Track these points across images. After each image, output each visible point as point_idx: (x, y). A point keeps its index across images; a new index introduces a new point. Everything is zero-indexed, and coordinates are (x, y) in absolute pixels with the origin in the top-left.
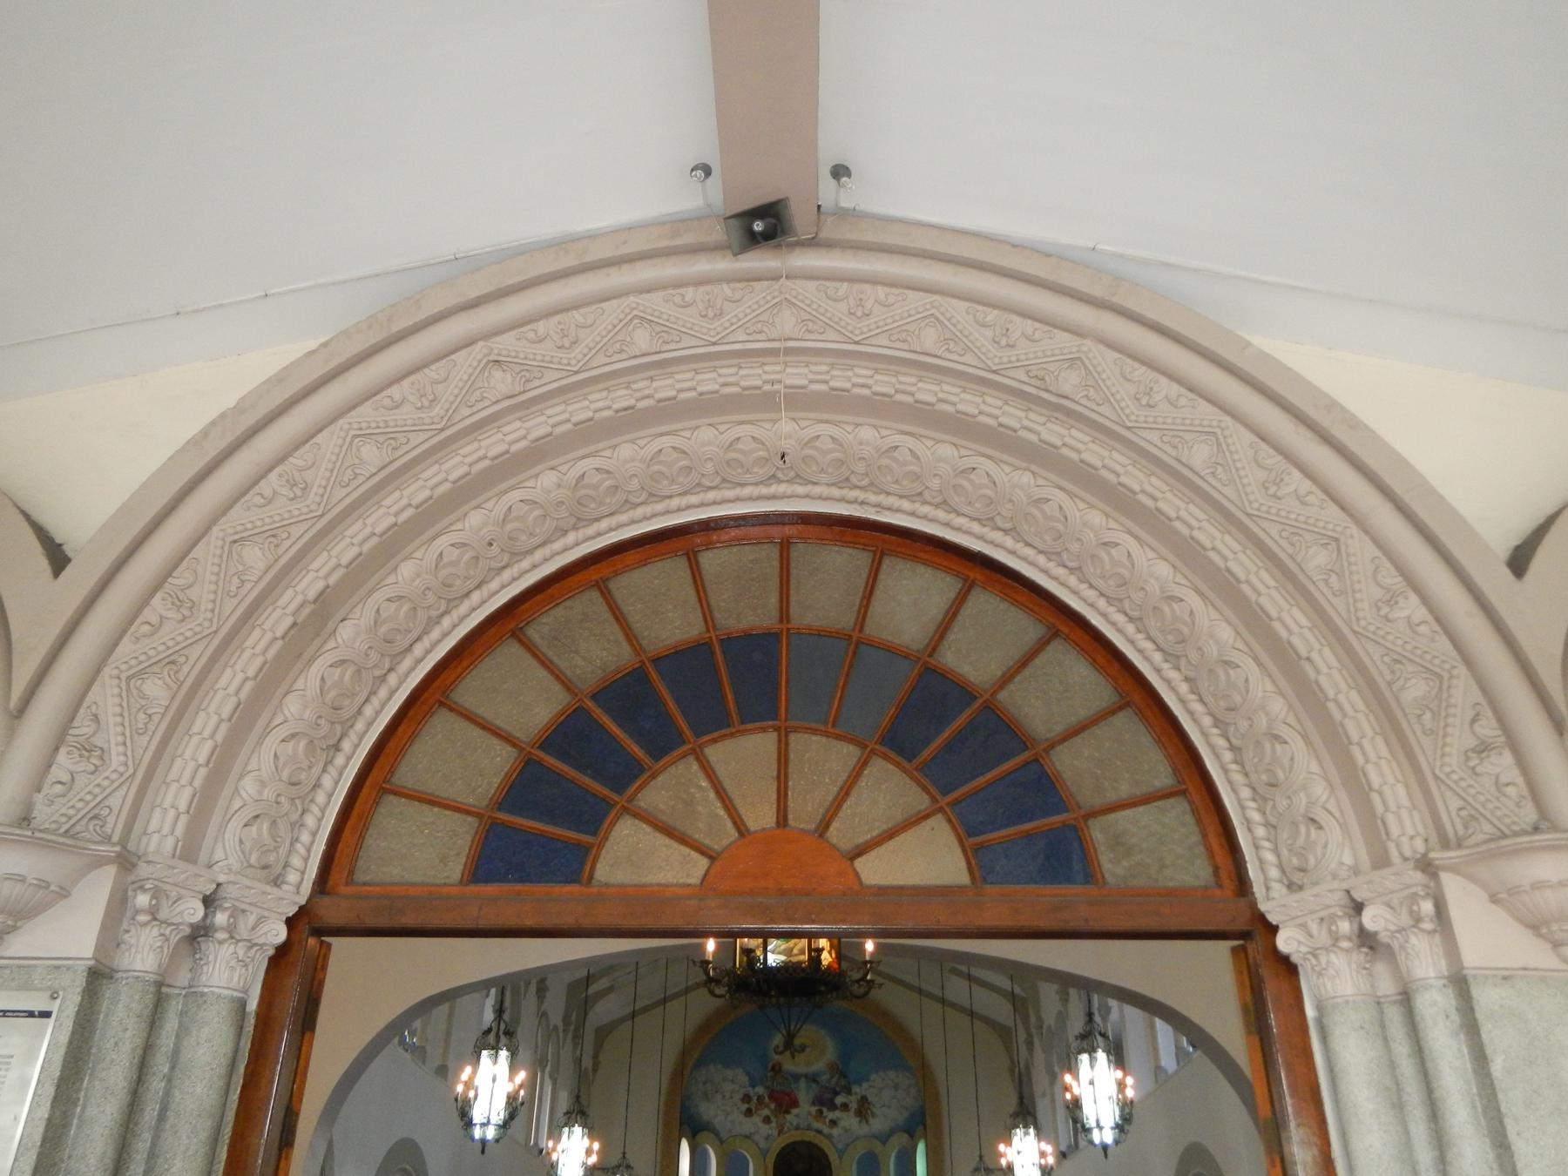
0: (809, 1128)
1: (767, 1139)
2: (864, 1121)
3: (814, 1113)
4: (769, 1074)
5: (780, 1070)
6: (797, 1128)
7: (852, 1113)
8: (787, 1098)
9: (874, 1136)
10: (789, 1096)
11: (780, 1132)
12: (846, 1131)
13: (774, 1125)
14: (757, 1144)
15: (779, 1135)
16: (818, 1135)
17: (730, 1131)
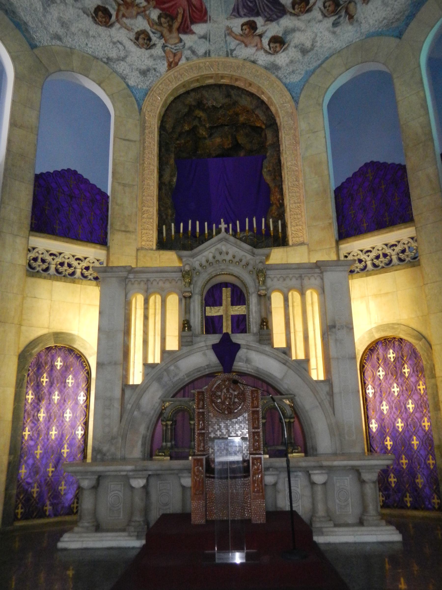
0: (230, 53)
1: (144, 73)
2: (344, 20)
3: (237, 30)
6: (207, 54)
7: (316, 13)
9: (370, 36)
11: (171, 65)
12: (304, 51)
13: (158, 51)
14: (124, 78)
16: (248, 64)
17: (58, 37)
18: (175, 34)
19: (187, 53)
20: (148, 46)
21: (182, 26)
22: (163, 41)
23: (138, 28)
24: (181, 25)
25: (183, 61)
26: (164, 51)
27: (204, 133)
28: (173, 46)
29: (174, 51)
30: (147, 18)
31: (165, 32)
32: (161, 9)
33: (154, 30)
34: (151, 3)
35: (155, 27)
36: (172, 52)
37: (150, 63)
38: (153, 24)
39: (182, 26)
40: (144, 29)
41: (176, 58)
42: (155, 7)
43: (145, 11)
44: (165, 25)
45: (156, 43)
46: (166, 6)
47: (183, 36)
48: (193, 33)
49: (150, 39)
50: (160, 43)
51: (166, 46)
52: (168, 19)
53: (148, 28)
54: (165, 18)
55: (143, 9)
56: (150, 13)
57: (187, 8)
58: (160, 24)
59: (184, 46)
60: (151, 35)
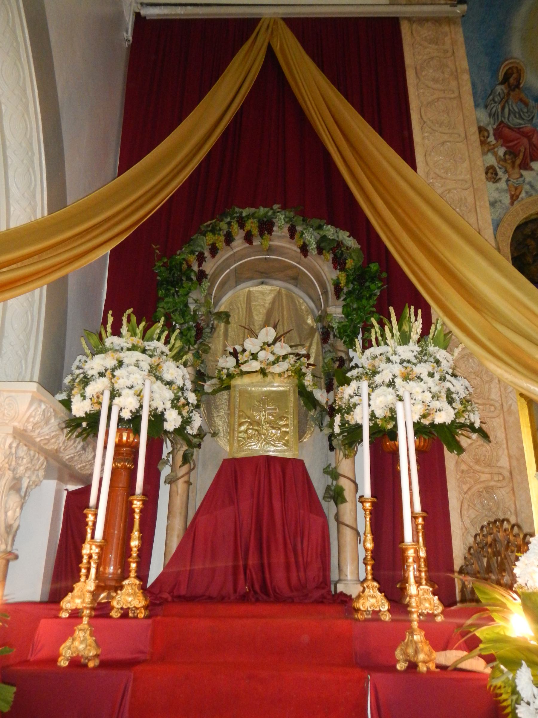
4: (499, 89)
5: (518, 86)
8: (525, 141)
10: (529, 138)
11: (514, 198)
13: (502, 185)
15: (512, 204)
18: (517, 170)
19: (527, 187)
20: (495, 179)
21: (523, 162)
22: (506, 176)
23: (488, 163)
24: (522, 162)
25: (523, 195)
26: (508, 185)
27: (530, 260)
28: (515, 181)
29: (515, 185)
30: (495, 154)
31: (509, 167)
32: (507, 147)
33: (500, 166)
34: (499, 141)
35: (501, 163)
36: (513, 185)
37: (496, 195)
38: (500, 161)
39: (523, 162)
40: (492, 164)
41: (517, 191)
42: (502, 146)
43: (494, 148)
44: (509, 162)
45: (502, 177)
46: (511, 144)
47: (524, 173)
48: (531, 169)
49: (496, 174)
50: (504, 177)
51: (509, 180)
52: (512, 156)
53: (495, 164)
54: (510, 155)
55: (492, 147)
56: (497, 151)
57: (528, 147)
58: (505, 160)
59: (524, 181)
60: (498, 170)
